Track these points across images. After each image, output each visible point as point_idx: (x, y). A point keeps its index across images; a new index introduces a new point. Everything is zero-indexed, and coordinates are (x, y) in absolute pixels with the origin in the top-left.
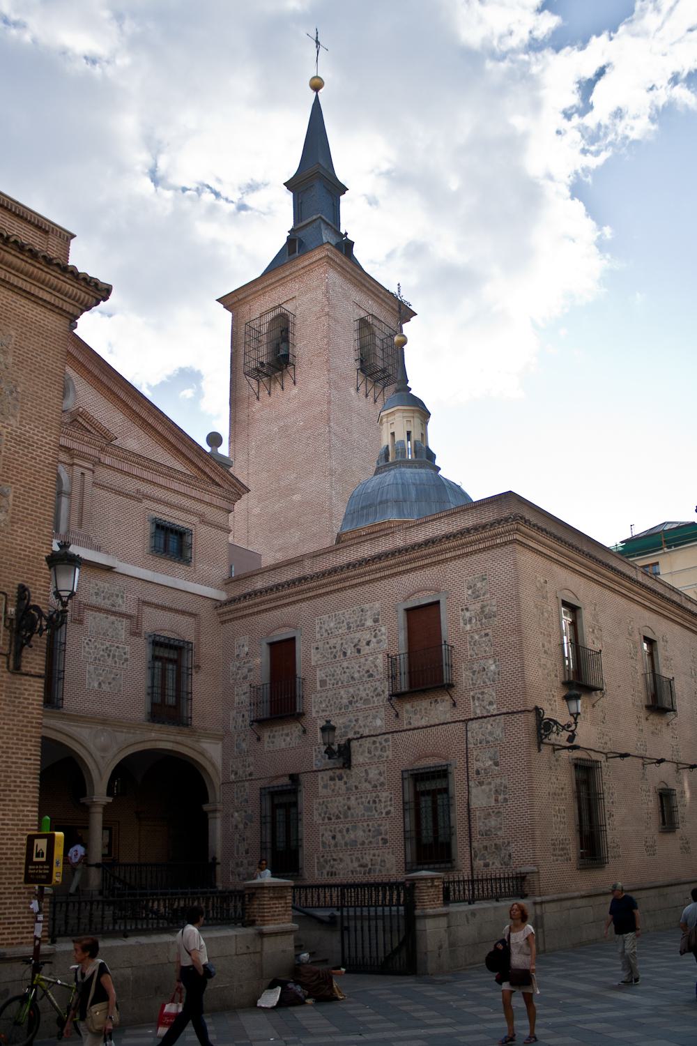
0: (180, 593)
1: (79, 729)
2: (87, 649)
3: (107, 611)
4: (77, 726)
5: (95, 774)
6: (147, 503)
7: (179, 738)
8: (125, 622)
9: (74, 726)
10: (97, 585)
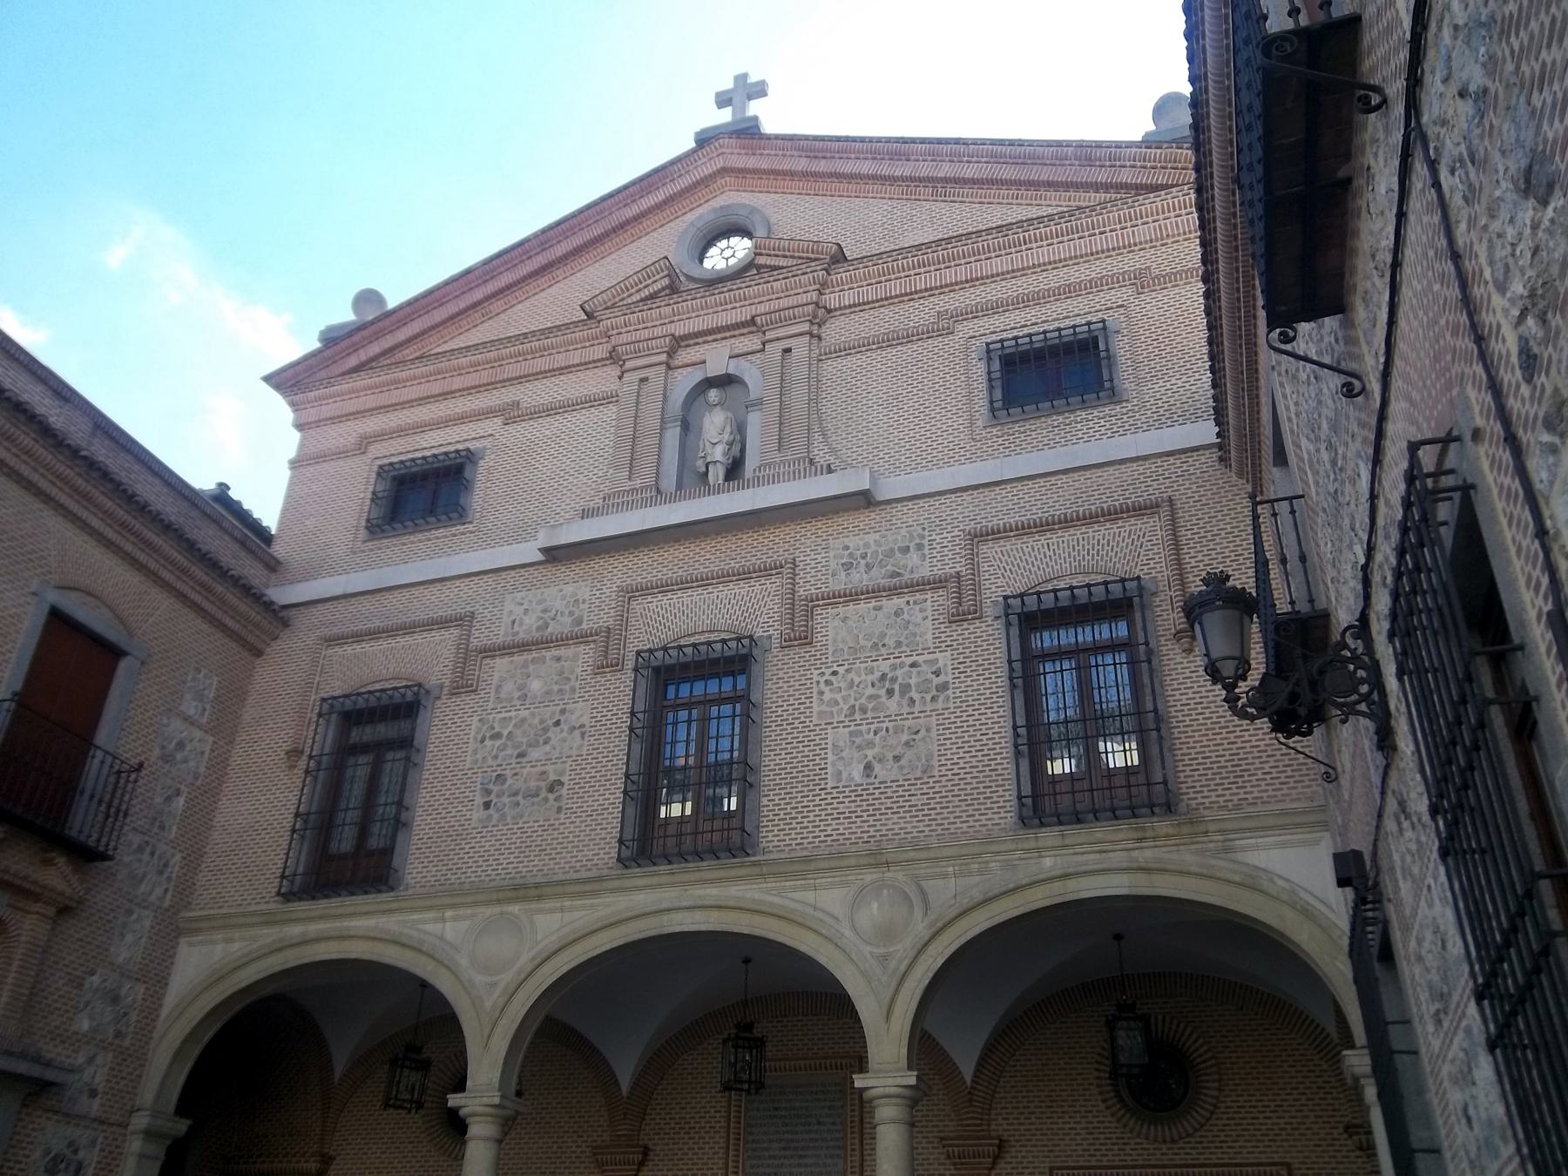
0: (1099, 472)
1: (810, 896)
2: (827, 697)
3: (874, 593)
4: (805, 888)
5: (867, 1009)
6: (965, 329)
7: (1146, 855)
8: (933, 601)
9: (795, 889)
10: (847, 548)
